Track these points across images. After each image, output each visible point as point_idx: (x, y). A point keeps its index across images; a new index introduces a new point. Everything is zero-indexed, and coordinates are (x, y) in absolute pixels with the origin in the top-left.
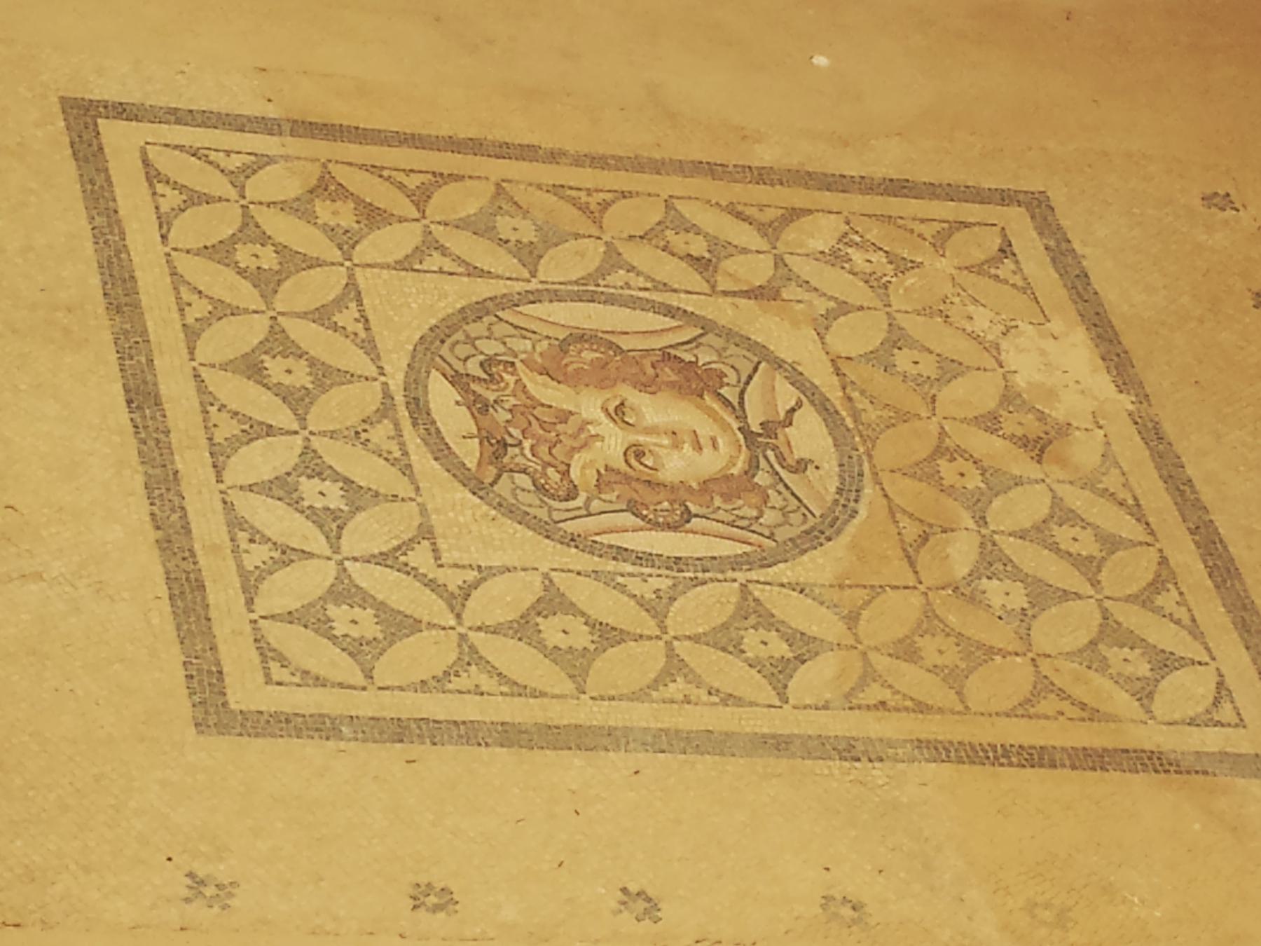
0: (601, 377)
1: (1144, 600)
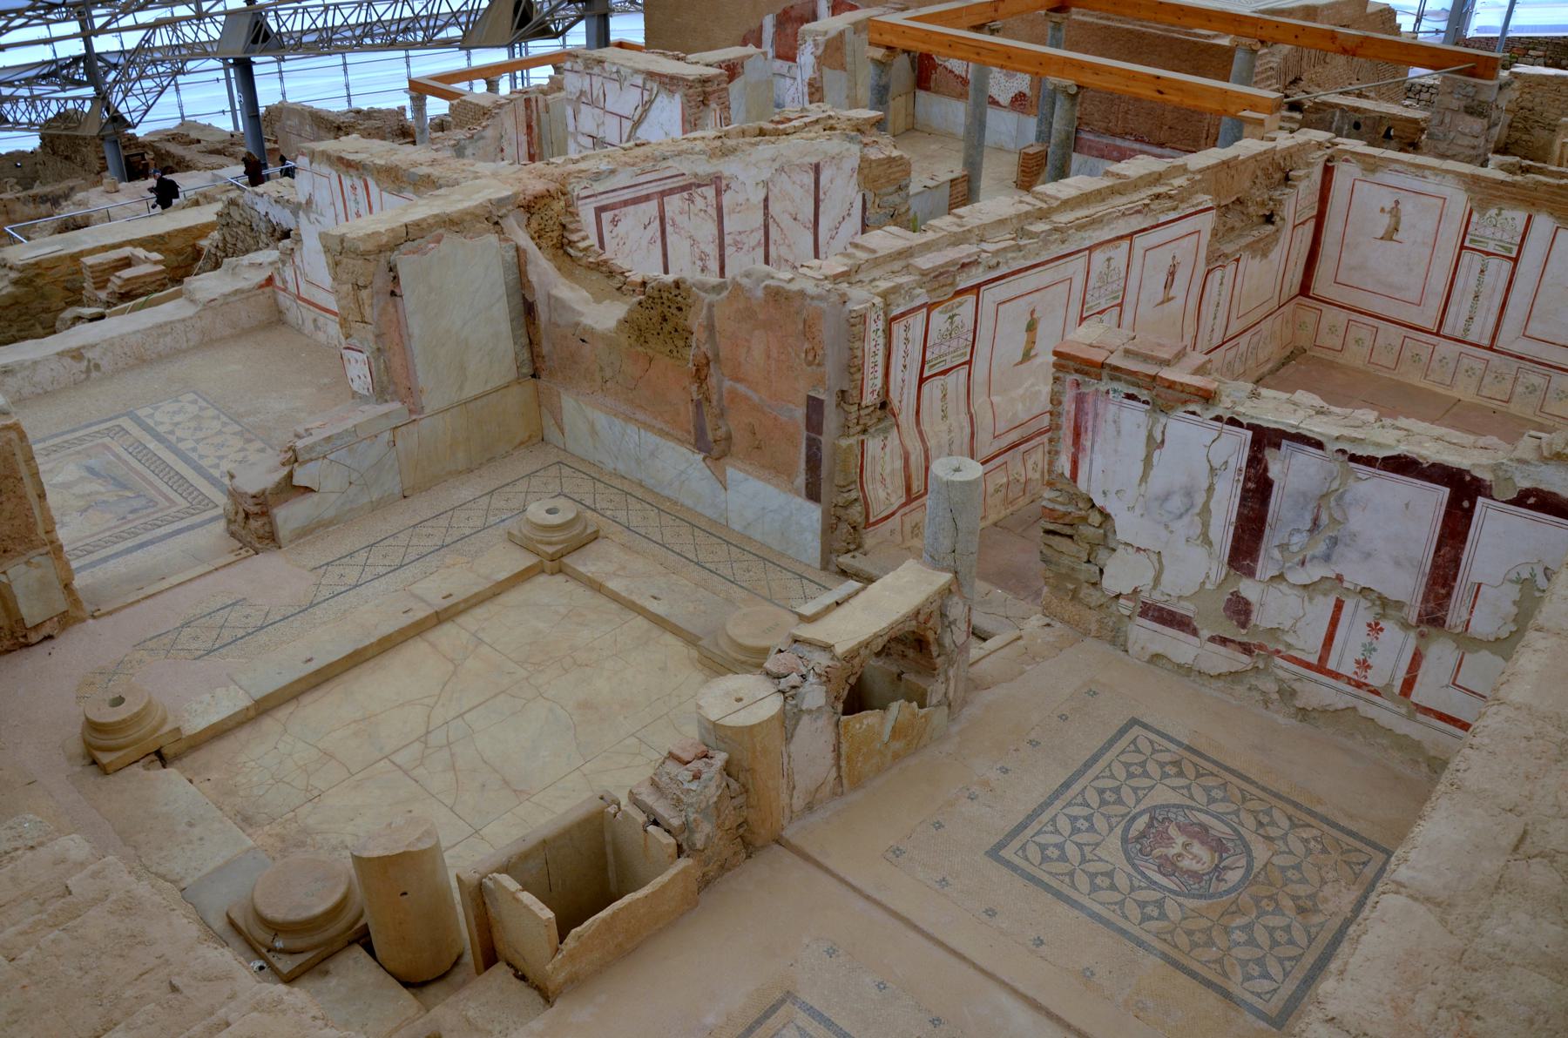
1: (1281, 961)
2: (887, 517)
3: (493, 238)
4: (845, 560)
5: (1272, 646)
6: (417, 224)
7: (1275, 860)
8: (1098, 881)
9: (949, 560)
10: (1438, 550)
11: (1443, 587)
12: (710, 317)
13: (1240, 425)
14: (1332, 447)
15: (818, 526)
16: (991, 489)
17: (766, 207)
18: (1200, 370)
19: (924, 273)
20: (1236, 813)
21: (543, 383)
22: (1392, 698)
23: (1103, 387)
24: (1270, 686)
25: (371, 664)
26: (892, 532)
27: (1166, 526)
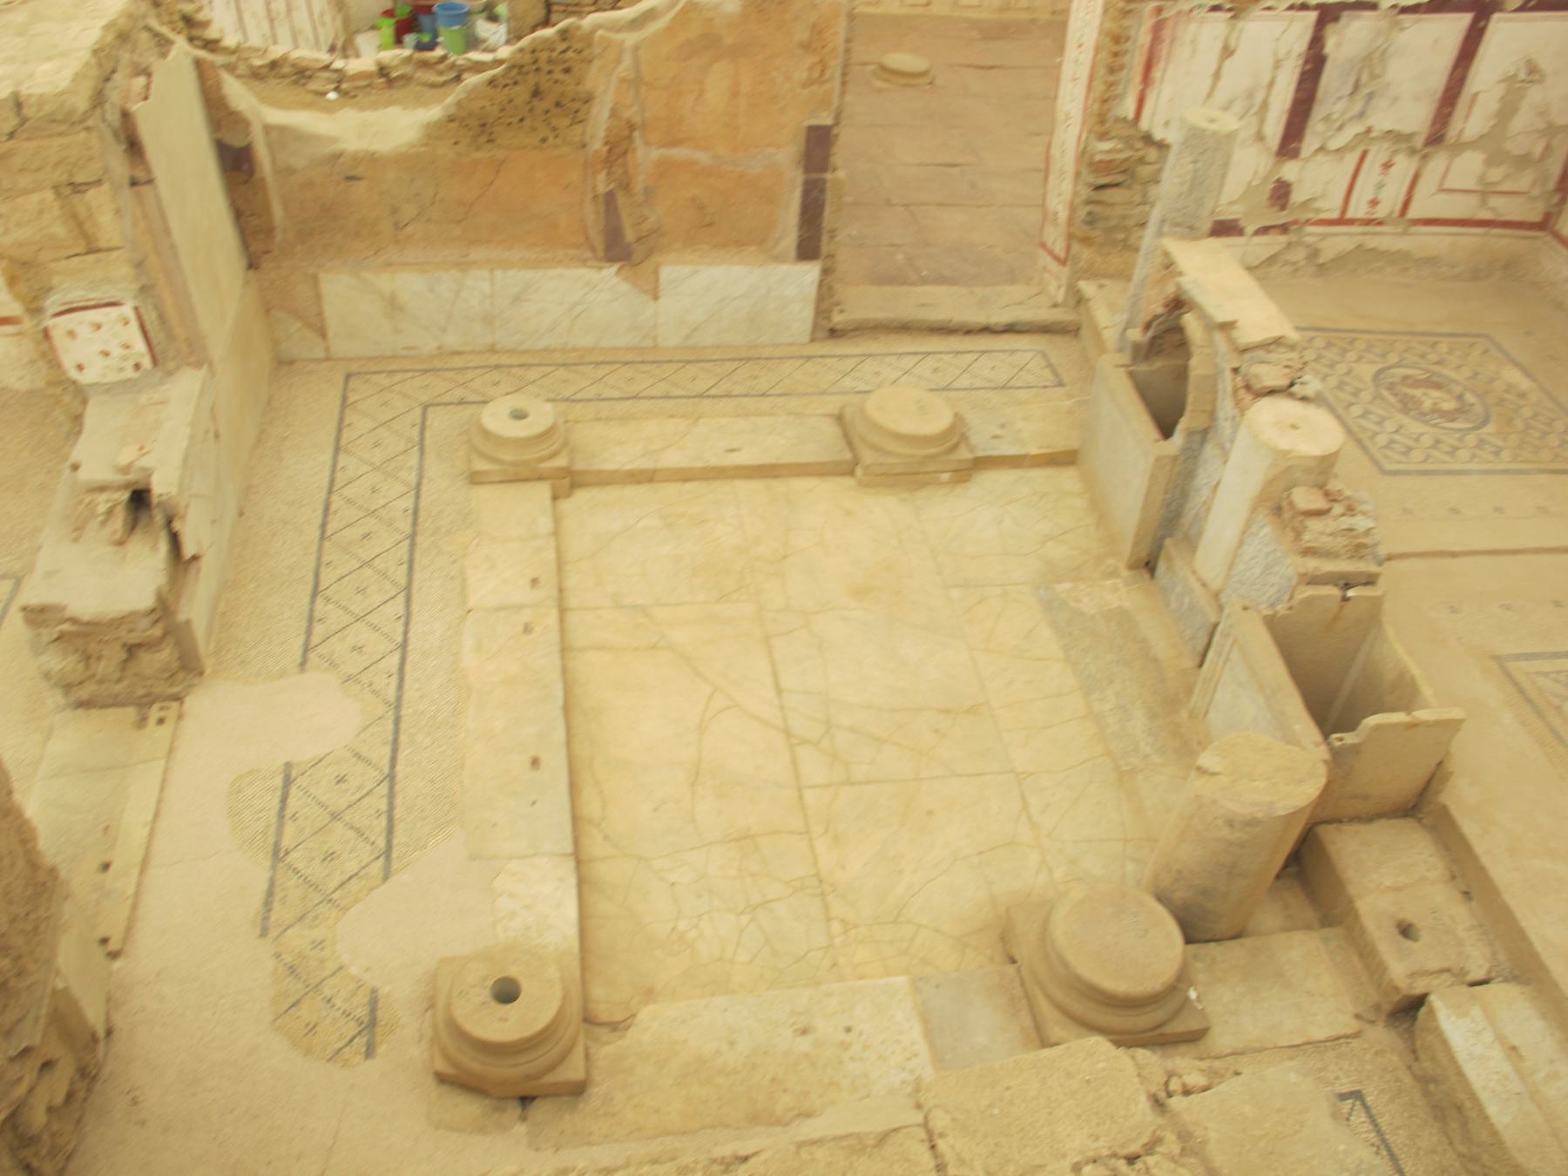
24: (1299, 255)
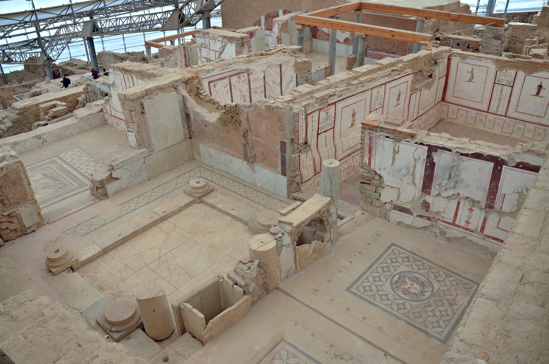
0: (413, 281)
1: (444, 321)
2: (309, 180)
3: (175, 93)
4: (295, 195)
5: (437, 218)
6: (149, 89)
7: (441, 288)
8: (383, 297)
9: (329, 194)
10: (491, 183)
11: (493, 195)
12: (247, 116)
13: (424, 145)
14: (454, 151)
15: (286, 184)
16: (342, 169)
17: (264, 79)
18: (410, 127)
19: (317, 99)
20: (428, 273)
21: (193, 140)
22: (477, 233)
23: (378, 134)
24: (437, 231)
25: (140, 235)
26: (310, 185)
27: (401, 179)
